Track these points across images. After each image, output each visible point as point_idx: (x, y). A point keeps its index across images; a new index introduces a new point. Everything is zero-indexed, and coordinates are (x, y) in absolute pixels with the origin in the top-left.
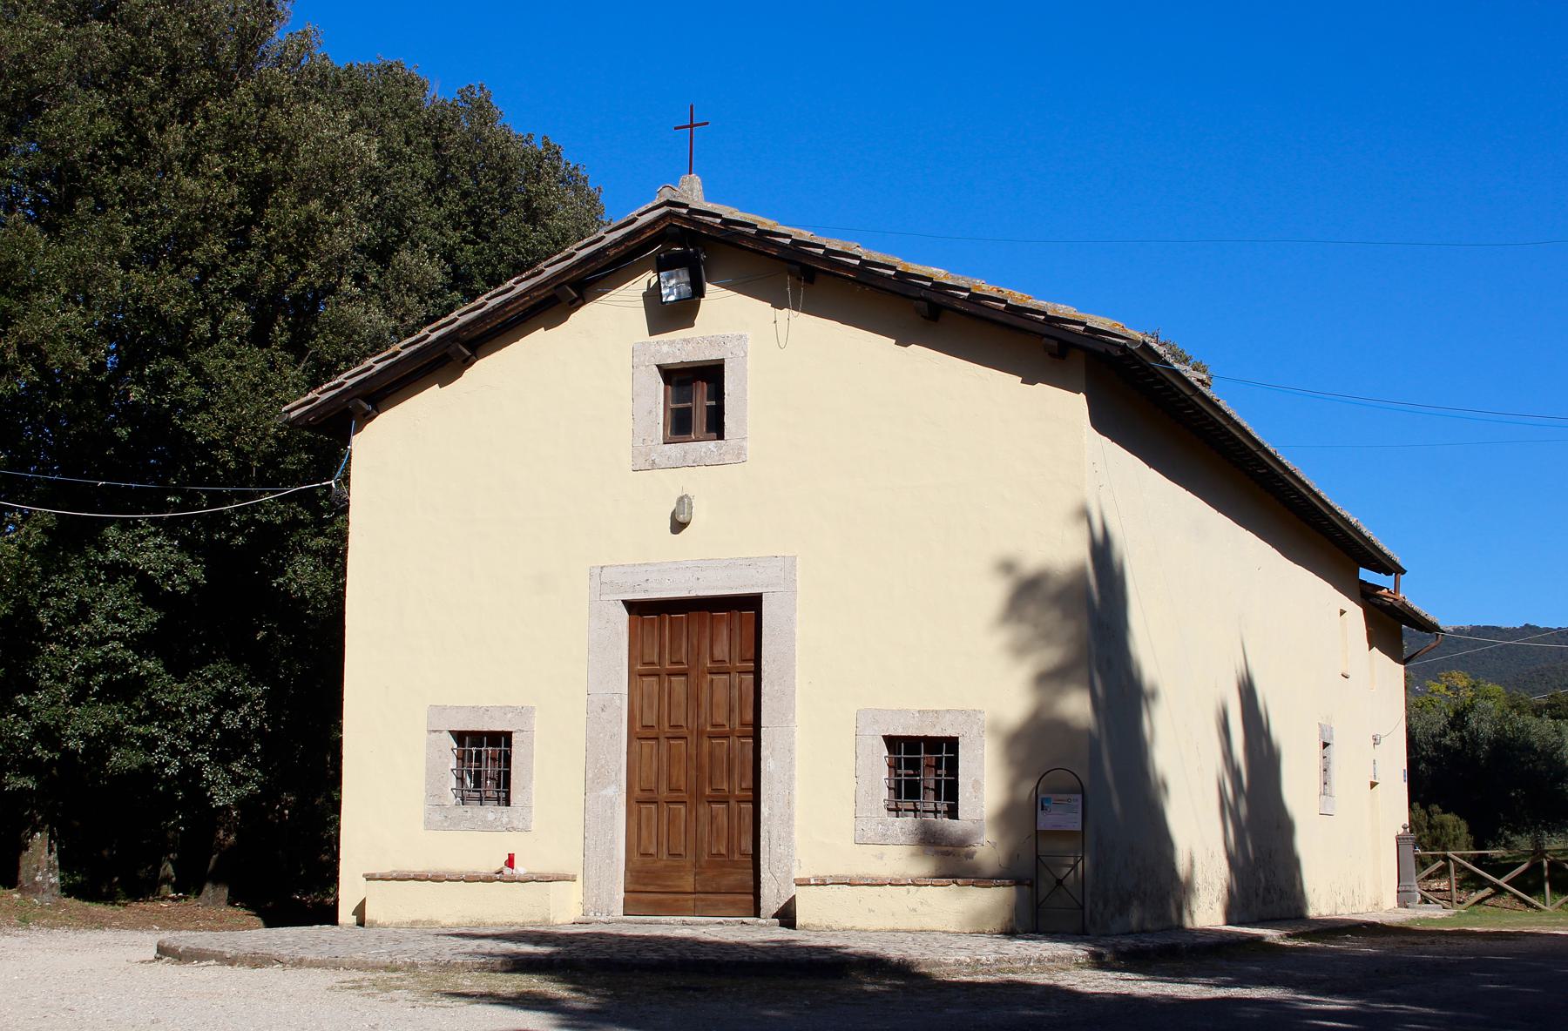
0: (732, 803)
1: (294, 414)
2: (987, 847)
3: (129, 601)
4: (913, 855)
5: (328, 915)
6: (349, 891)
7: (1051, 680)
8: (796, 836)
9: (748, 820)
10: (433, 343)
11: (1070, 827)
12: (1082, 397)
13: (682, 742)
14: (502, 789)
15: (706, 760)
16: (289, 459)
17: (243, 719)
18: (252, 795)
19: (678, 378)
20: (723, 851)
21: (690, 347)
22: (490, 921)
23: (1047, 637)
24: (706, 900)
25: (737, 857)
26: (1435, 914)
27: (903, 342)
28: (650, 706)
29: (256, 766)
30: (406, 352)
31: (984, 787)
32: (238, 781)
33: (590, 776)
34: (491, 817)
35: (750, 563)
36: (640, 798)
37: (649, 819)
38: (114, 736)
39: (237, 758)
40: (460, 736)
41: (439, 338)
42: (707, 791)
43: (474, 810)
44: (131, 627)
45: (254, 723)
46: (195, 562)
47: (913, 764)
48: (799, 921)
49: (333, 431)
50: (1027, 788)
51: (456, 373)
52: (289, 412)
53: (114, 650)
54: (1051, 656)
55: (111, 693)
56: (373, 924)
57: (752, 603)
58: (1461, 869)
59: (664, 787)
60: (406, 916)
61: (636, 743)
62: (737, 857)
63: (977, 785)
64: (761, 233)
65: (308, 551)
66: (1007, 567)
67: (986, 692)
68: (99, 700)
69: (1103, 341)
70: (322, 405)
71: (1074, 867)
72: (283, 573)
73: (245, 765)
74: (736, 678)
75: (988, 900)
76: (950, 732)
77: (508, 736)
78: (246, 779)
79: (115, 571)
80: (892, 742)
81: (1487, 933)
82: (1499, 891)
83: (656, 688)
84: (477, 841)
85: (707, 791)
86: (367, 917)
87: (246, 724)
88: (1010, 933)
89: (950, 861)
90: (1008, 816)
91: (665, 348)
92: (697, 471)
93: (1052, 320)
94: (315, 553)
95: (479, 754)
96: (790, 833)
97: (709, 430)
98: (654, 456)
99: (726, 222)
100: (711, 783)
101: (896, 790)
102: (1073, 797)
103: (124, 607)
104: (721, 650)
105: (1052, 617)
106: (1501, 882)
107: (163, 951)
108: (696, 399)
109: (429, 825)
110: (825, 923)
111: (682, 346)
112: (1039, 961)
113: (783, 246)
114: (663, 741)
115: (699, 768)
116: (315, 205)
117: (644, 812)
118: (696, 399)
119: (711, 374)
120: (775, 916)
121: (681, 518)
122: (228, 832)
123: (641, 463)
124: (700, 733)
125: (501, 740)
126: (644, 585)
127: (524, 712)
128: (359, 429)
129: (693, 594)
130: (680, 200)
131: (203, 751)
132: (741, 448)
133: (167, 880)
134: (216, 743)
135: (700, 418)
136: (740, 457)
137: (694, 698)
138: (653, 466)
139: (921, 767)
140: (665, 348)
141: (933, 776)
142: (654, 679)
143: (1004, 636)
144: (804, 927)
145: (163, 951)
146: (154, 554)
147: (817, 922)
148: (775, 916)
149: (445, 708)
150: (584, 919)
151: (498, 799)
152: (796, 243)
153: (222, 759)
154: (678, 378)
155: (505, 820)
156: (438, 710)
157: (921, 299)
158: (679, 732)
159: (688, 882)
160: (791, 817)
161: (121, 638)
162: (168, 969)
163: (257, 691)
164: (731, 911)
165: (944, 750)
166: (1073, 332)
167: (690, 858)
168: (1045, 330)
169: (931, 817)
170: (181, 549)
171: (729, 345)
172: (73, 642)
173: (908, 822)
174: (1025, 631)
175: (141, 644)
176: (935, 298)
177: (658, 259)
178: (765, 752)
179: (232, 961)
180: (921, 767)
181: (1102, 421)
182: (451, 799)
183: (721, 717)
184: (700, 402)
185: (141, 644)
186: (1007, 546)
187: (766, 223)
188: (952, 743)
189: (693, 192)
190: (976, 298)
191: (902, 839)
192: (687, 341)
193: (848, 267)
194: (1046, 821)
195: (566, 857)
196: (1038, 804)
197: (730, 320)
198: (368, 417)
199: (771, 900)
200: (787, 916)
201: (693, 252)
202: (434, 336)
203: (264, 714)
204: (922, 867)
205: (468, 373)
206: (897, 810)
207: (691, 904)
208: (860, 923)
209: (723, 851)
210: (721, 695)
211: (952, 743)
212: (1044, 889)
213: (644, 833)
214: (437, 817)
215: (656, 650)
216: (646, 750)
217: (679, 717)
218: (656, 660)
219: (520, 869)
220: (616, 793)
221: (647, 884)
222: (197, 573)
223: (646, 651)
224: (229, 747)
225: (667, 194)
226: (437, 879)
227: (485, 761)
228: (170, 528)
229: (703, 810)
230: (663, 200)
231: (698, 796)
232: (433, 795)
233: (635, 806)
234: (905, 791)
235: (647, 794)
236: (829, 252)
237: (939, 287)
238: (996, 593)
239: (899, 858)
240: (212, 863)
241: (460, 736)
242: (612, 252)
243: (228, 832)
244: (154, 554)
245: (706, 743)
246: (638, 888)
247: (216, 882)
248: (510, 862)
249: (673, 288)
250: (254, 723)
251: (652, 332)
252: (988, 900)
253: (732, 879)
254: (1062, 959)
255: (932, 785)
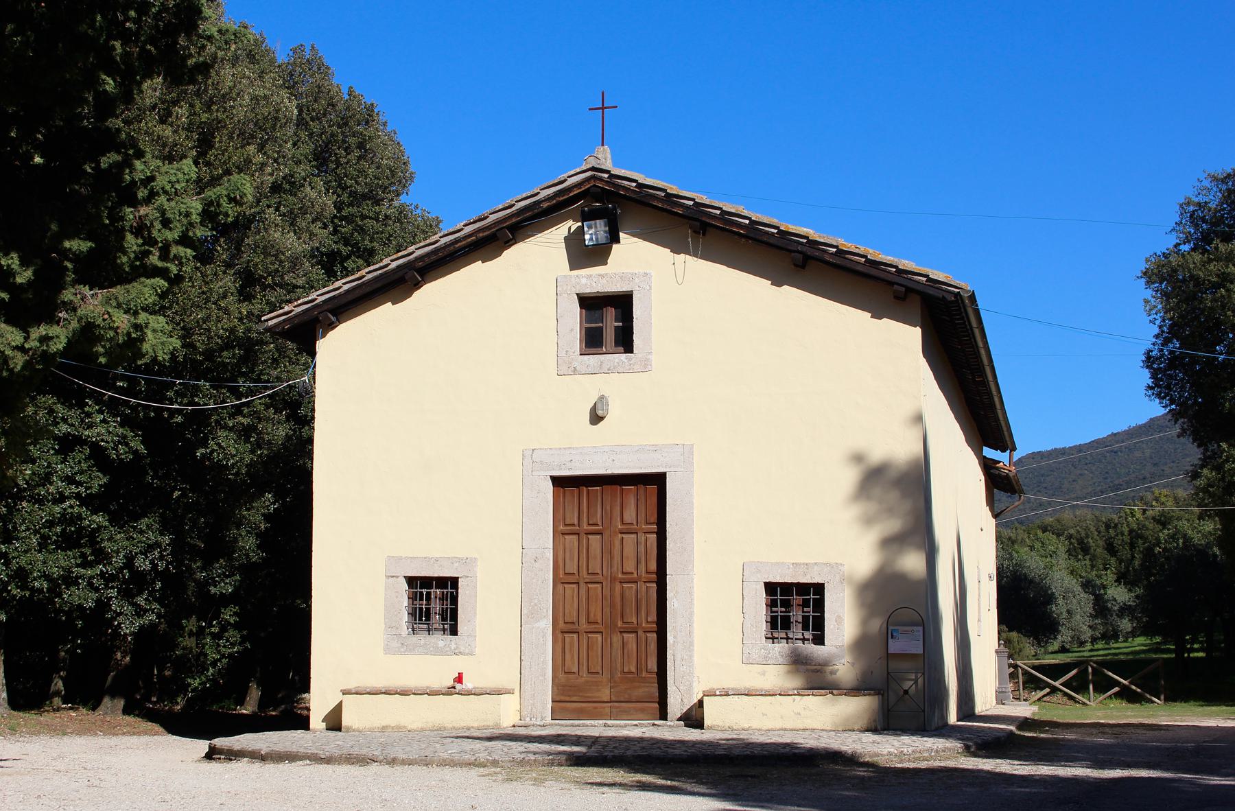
0: (640, 633)
1: (271, 323)
2: (845, 669)
3: (84, 466)
4: (789, 672)
5: (302, 723)
6: (319, 702)
7: (892, 543)
8: (696, 658)
9: (653, 647)
10: (393, 270)
11: (914, 651)
12: (918, 331)
13: (599, 586)
14: (451, 623)
15: (618, 599)
16: (225, 354)
17: (152, 562)
18: (153, 626)
19: (590, 304)
20: (633, 670)
21: (604, 281)
22: (449, 726)
23: (890, 511)
24: (620, 707)
25: (644, 674)
26: (1024, 710)
27: (777, 283)
28: (572, 559)
29: (156, 600)
30: (370, 276)
31: (843, 621)
32: (140, 612)
33: (524, 612)
34: (441, 644)
35: (656, 449)
36: (564, 629)
37: (571, 644)
38: (69, 580)
39: (140, 593)
40: (411, 581)
41: (398, 267)
42: (620, 624)
43: (423, 638)
44: (87, 488)
45: (161, 566)
46: (137, 435)
47: (787, 604)
48: (707, 722)
49: (305, 335)
50: (876, 625)
51: (408, 294)
52: (267, 320)
53: (71, 507)
54: (893, 525)
55: (68, 542)
56: (348, 730)
57: (658, 480)
58: (1025, 673)
59: (583, 620)
60: (378, 722)
61: (560, 587)
62: (644, 674)
63: (839, 620)
64: (669, 196)
65: (225, 427)
66: (858, 458)
67: (843, 551)
68: (57, 548)
69: (941, 289)
70: (297, 316)
71: (916, 682)
72: (204, 444)
73: (146, 600)
74: (642, 537)
75: (856, 707)
76: (817, 580)
77: (454, 581)
78: (146, 611)
79: (67, 445)
80: (770, 588)
81: (1148, 725)
82: (1054, 690)
83: (576, 544)
84: (432, 661)
85: (620, 624)
86: (344, 724)
87: (154, 566)
88: (874, 730)
89: (815, 679)
90: (861, 645)
91: (584, 281)
92: (608, 376)
93: (901, 272)
94: (231, 429)
95: (429, 594)
96: (691, 656)
97: (617, 344)
98: (575, 364)
99: (640, 186)
100: (622, 616)
101: (773, 623)
102: (915, 628)
103: (81, 472)
104: (630, 515)
105: (893, 496)
106: (1057, 684)
107: (211, 755)
108: (609, 322)
109: (387, 650)
110: (727, 725)
111: (596, 280)
112: (937, 751)
113: (687, 207)
114: (583, 587)
115: (612, 605)
116: (252, 149)
117: (567, 640)
118: (609, 322)
119: (622, 303)
120: (680, 719)
121: (600, 413)
122: (125, 654)
123: (564, 369)
124: (613, 579)
125: (449, 585)
126: (569, 465)
127: (468, 562)
128: (323, 336)
129: (609, 472)
130: (603, 167)
131: (113, 588)
132: (647, 360)
133: (57, 693)
134: (125, 581)
135: (609, 336)
136: (646, 366)
137: (607, 551)
138: (575, 372)
139: (793, 606)
140: (584, 281)
141: (800, 613)
142: (575, 537)
143: (855, 510)
144: (710, 728)
145: (211, 755)
146: (104, 430)
147: (721, 724)
148: (680, 719)
149: (400, 558)
150: (522, 723)
151: (444, 630)
152: (697, 204)
153: (127, 595)
154: (590, 304)
155: (453, 646)
156: (393, 560)
157: (798, 252)
158: (571, 579)
159: (605, 694)
160: (691, 644)
161: (78, 496)
162: (214, 766)
163: (167, 539)
164: (641, 716)
165: (813, 595)
166: (918, 282)
167: (607, 675)
168: (896, 279)
169: (800, 644)
170: (122, 425)
171: (637, 280)
172: (40, 501)
173: (781, 648)
174: (872, 507)
175: (92, 502)
176: (809, 251)
177: (583, 212)
178: (670, 594)
179: (328, 761)
180: (793, 606)
181: (927, 352)
182: (404, 629)
183: (630, 566)
184: (610, 323)
185: (92, 502)
186: (860, 442)
187: (673, 189)
188: (819, 588)
189: (605, 159)
190: (841, 253)
191: (781, 660)
192: (602, 276)
193: (740, 225)
194: (895, 647)
195: (509, 678)
196: (888, 634)
197: (636, 262)
198: (331, 326)
199: (677, 703)
200: (693, 718)
201: (607, 207)
202: (394, 265)
203: (170, 558)
204: (795, 682)
205: (417, 294)
206: (773, 638)
207: (608, 710)
208: (755, 724)
209: (633, 670)
210: (630, 550)
211: (819, 588)
212: (893, 699)
213: (568, 656)
214: (395, 644)
215: (576, 515)
216: (568, 592)
217: (595, 566)
218: (576, 522)
219: (468, 684)
220: (546, 624)
221: (568, 697)
222: (137, 444)
223: (568, 515)
224: (133, 583)
225: (592, 162)
226: (404, 693)
227: (434, 601)
228: (113, 407)
229: (617, 639)
230: (589, 166)
231: (612, 627)
232: (390, 626)
233: (560, 636)
234: (778, 624)
235: (570, 627)
236: (724, 213)
237: (813, 243)
238: (849, 477)
239: (774, 674)
240: (110, 678)
241: (411, 581)
242: (545, 205)
243: (125, 654)
244: (104, 430)
245: (618, 587)
246: (563, 698)
247: (113, 696)
248: (459, 679)
249: (594, 233)
250: (161, 566)
251: (571, 269)
252: (856, 707)
253: (640, 692)
254: (950, 749)
255: (800, 620)
